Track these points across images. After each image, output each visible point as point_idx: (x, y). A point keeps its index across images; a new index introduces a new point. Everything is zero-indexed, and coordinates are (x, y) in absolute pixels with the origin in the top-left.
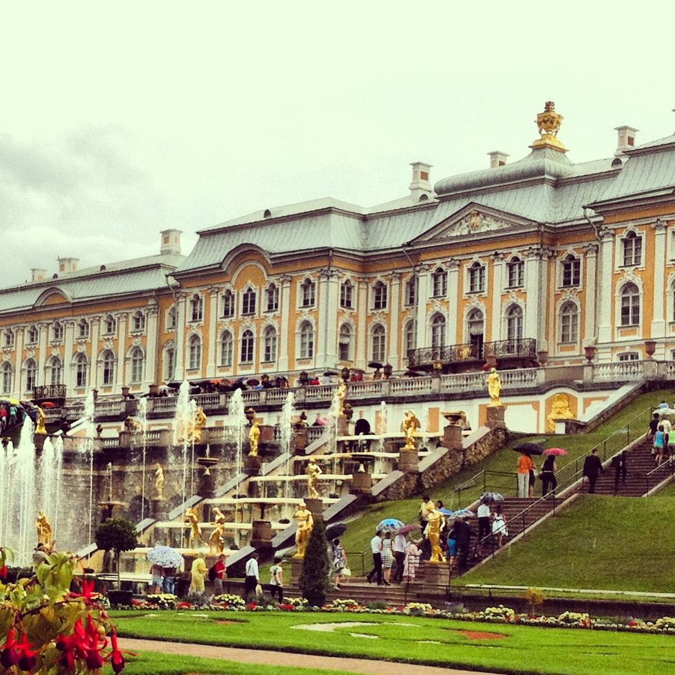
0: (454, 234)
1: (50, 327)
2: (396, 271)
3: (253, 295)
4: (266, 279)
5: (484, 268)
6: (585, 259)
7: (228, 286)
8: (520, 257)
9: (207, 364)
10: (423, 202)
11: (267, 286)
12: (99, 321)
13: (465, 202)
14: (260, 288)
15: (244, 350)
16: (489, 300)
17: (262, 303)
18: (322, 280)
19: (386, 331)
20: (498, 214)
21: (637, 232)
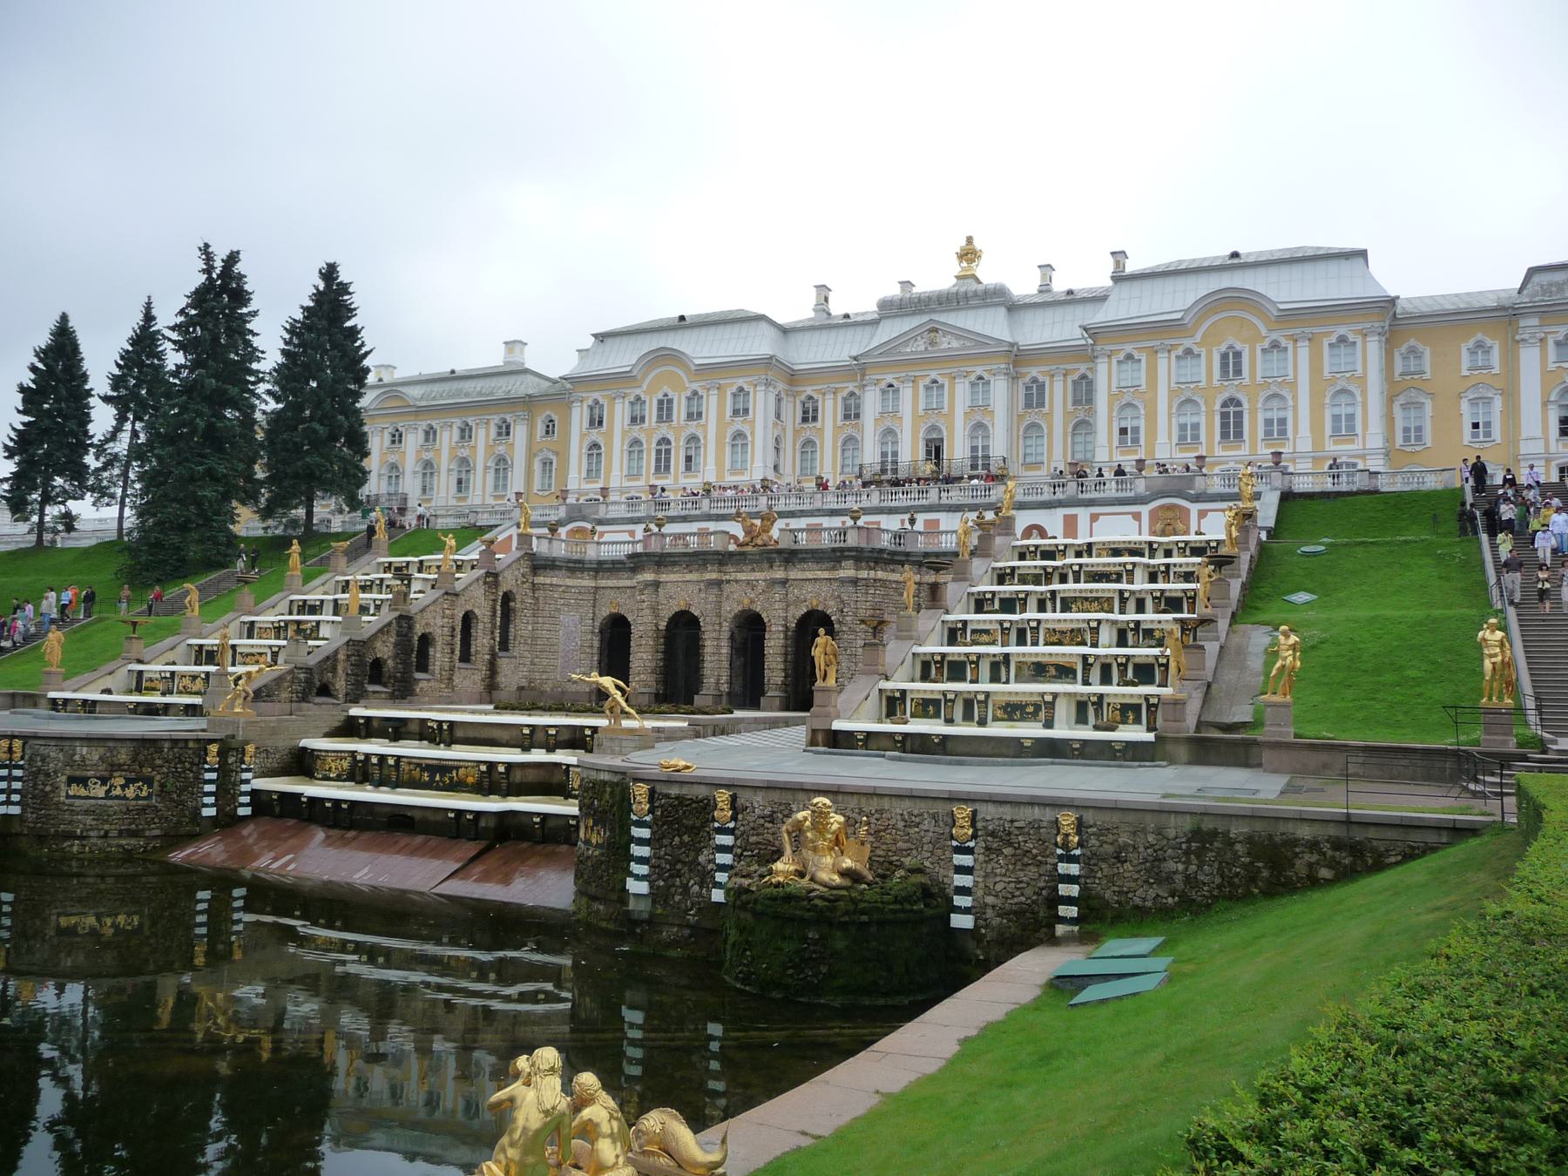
0: (908, 350)
1: (385, 431)
3: (670, 401)
5: (942, 386)
7: (638, 391)
8: (986, 376)
9: (610, 472)
10: (845, 321)
12: (451, 426)
14: (680, 396)
15: (658, 460)
16: (950, 416)
17: (680, 411)
19: (818, 446)
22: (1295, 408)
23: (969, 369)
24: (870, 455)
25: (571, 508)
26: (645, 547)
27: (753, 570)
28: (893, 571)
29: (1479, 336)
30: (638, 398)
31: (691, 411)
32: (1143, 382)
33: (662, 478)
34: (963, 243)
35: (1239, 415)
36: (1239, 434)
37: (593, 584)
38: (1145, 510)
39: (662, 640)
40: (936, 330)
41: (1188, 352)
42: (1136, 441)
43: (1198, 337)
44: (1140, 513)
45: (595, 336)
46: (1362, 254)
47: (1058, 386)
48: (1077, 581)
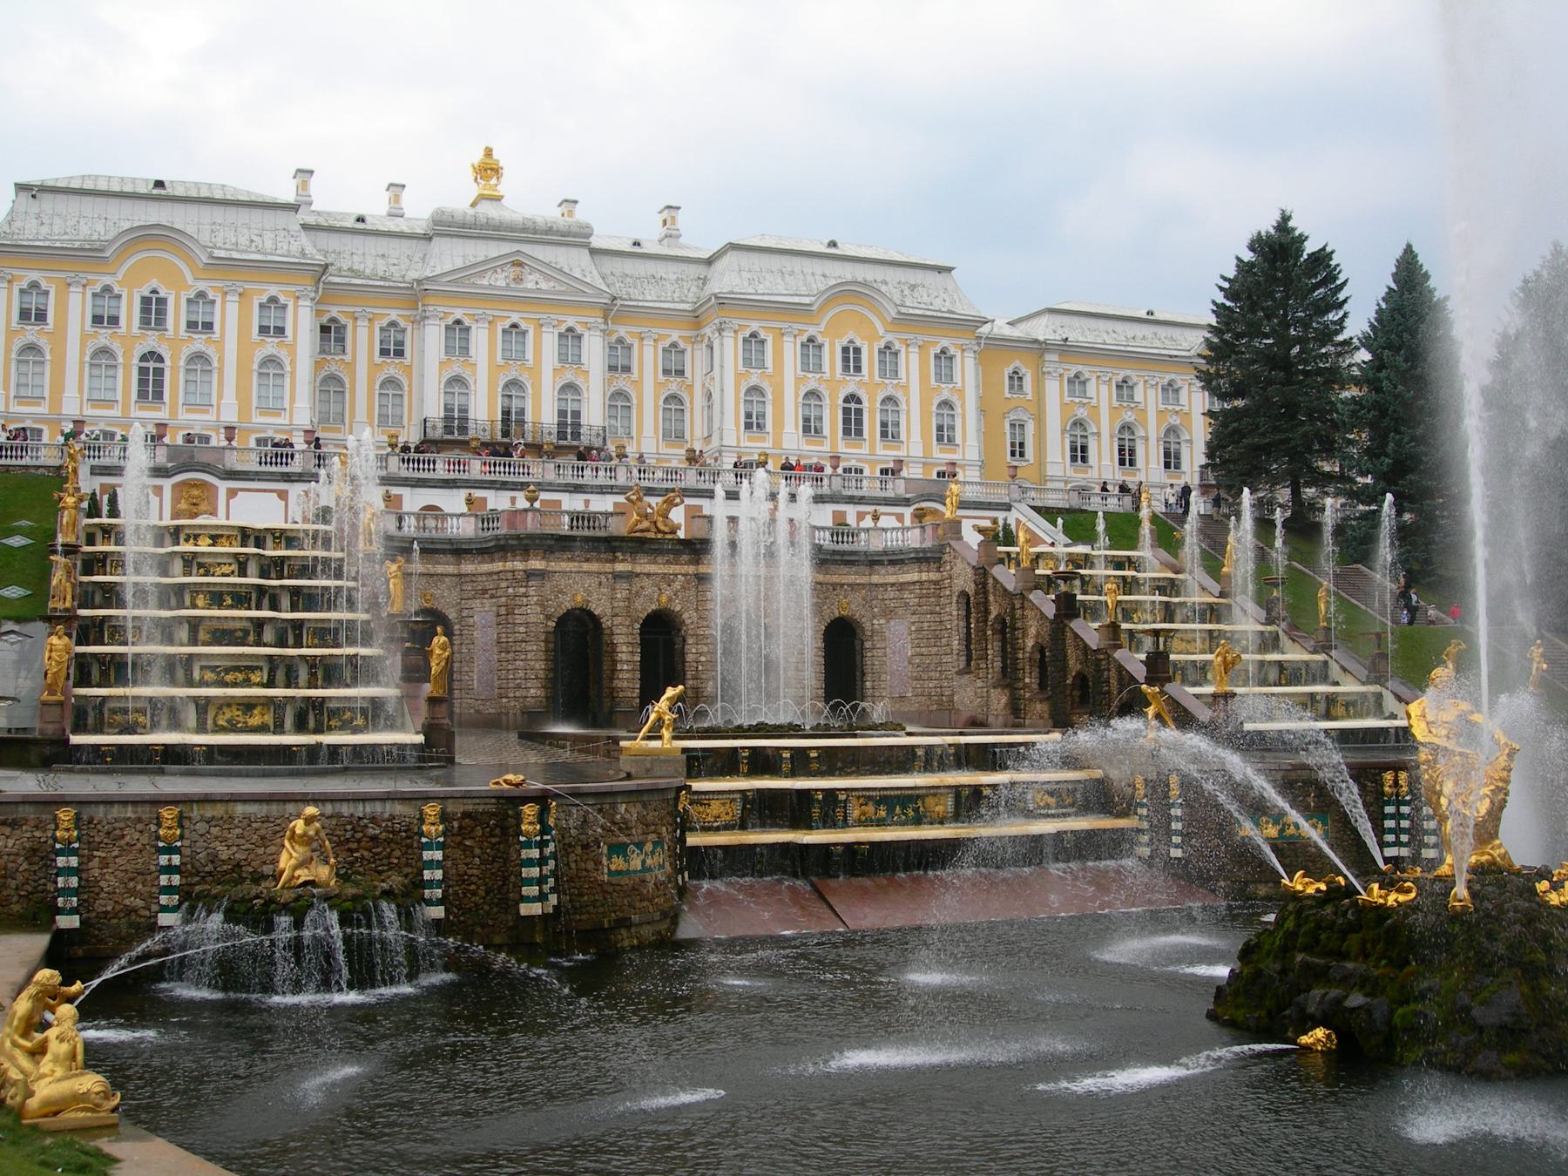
0: (485, 282)
2: (368, 310)
3: (162, 302)
4: (190, 283)
5: (524, 333)
6: (641, 347)
7: (107, 280)
8: (579, 330)
13: (494, 250)
15: (143, 382)
16: (536, 371)
17: (176, 316)
18: (301, 302)
19: (347, 386)
20: (551, 271)
21: (762, 335)
22: (908, 411)
23: (561, 318)
25: (173, 451)
26: (511, 524)
27: (668, 562)
29: (1017, 363)
30: (107, 289)
31: (193, 318)
33: (155, 409)
35: (859, 412)
36: (859, 432)
39: (551, 646)
40: (520, 264)
41: (811, 340)
44: (903, 515)
45: (21, 188)
46: (949, 270)
47: (649, 352)
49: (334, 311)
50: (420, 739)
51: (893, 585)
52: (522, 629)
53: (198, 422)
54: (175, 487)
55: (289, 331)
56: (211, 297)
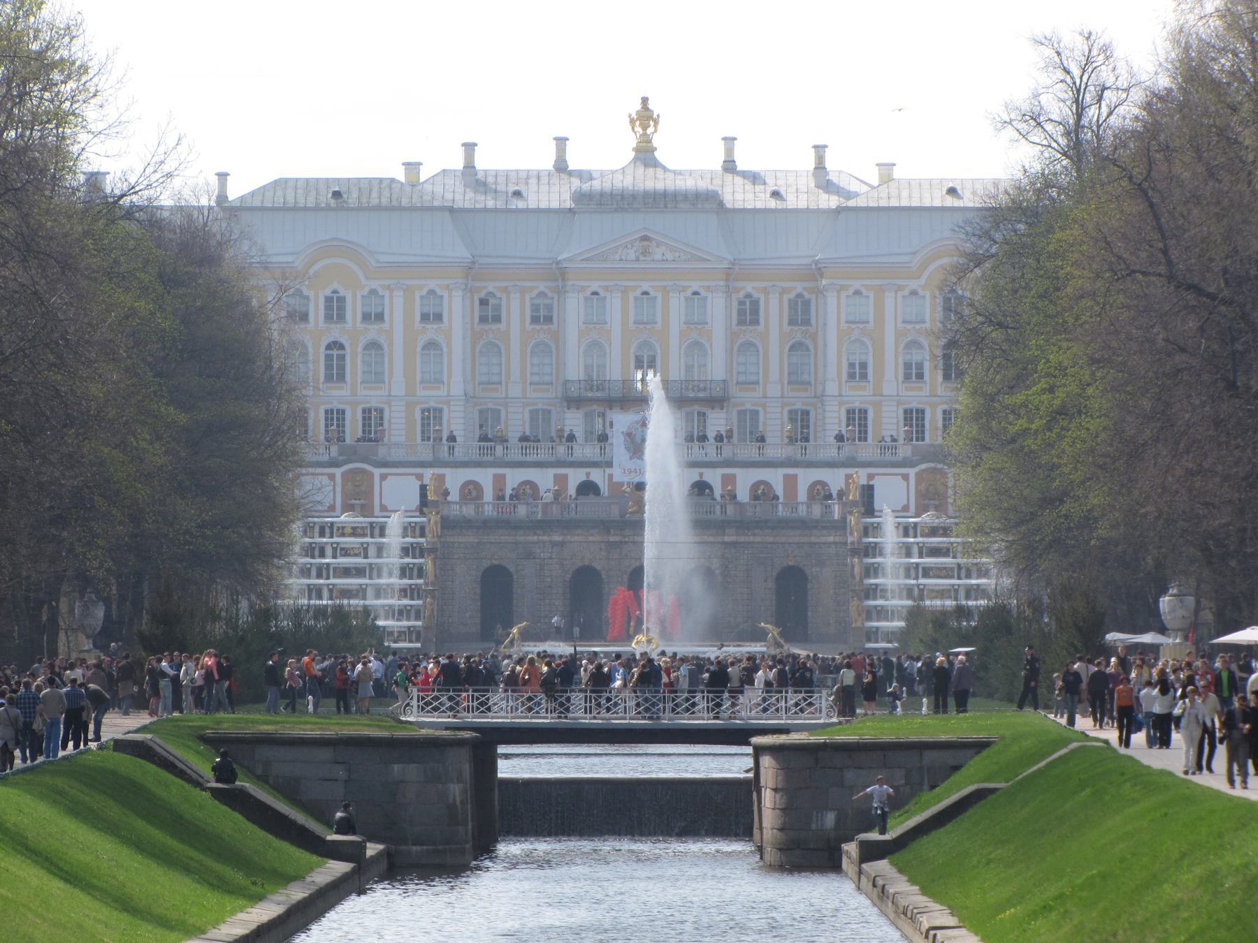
0: (617, 257)
2: (519, 283)
3: (342, 300)
11: (366, 292)
14: (354, 296)
15: (328, 367)
17: (354, 311)
19: (503, 351)
21: (865, 292)
23: (686, 284)
24: (574, 370)
26: (544, 512)
28: (754, 535)
32: (871, 319)
34: (639, 107)
37: (477, 541)
38: (912, 472)
42: (864, 376)
43: (922, 281)
48: (921, 556)
49: (491, 289)
50: (419, 645)
51: (824, 543)
52: (549, 580)
53: (374, 397)
54: (343, 474)
55: (445, 318)
56: (381, 294)
